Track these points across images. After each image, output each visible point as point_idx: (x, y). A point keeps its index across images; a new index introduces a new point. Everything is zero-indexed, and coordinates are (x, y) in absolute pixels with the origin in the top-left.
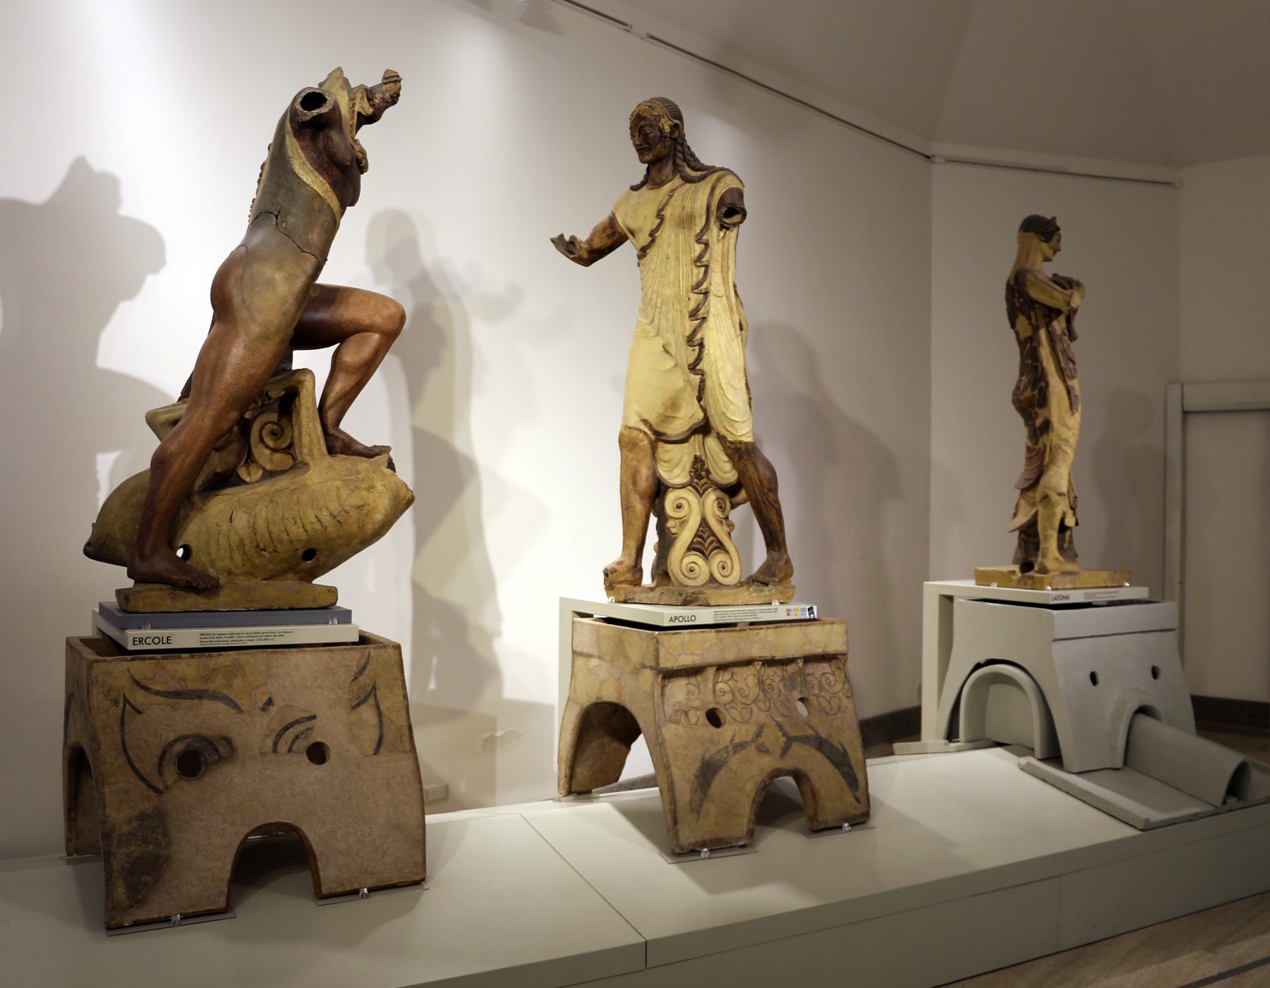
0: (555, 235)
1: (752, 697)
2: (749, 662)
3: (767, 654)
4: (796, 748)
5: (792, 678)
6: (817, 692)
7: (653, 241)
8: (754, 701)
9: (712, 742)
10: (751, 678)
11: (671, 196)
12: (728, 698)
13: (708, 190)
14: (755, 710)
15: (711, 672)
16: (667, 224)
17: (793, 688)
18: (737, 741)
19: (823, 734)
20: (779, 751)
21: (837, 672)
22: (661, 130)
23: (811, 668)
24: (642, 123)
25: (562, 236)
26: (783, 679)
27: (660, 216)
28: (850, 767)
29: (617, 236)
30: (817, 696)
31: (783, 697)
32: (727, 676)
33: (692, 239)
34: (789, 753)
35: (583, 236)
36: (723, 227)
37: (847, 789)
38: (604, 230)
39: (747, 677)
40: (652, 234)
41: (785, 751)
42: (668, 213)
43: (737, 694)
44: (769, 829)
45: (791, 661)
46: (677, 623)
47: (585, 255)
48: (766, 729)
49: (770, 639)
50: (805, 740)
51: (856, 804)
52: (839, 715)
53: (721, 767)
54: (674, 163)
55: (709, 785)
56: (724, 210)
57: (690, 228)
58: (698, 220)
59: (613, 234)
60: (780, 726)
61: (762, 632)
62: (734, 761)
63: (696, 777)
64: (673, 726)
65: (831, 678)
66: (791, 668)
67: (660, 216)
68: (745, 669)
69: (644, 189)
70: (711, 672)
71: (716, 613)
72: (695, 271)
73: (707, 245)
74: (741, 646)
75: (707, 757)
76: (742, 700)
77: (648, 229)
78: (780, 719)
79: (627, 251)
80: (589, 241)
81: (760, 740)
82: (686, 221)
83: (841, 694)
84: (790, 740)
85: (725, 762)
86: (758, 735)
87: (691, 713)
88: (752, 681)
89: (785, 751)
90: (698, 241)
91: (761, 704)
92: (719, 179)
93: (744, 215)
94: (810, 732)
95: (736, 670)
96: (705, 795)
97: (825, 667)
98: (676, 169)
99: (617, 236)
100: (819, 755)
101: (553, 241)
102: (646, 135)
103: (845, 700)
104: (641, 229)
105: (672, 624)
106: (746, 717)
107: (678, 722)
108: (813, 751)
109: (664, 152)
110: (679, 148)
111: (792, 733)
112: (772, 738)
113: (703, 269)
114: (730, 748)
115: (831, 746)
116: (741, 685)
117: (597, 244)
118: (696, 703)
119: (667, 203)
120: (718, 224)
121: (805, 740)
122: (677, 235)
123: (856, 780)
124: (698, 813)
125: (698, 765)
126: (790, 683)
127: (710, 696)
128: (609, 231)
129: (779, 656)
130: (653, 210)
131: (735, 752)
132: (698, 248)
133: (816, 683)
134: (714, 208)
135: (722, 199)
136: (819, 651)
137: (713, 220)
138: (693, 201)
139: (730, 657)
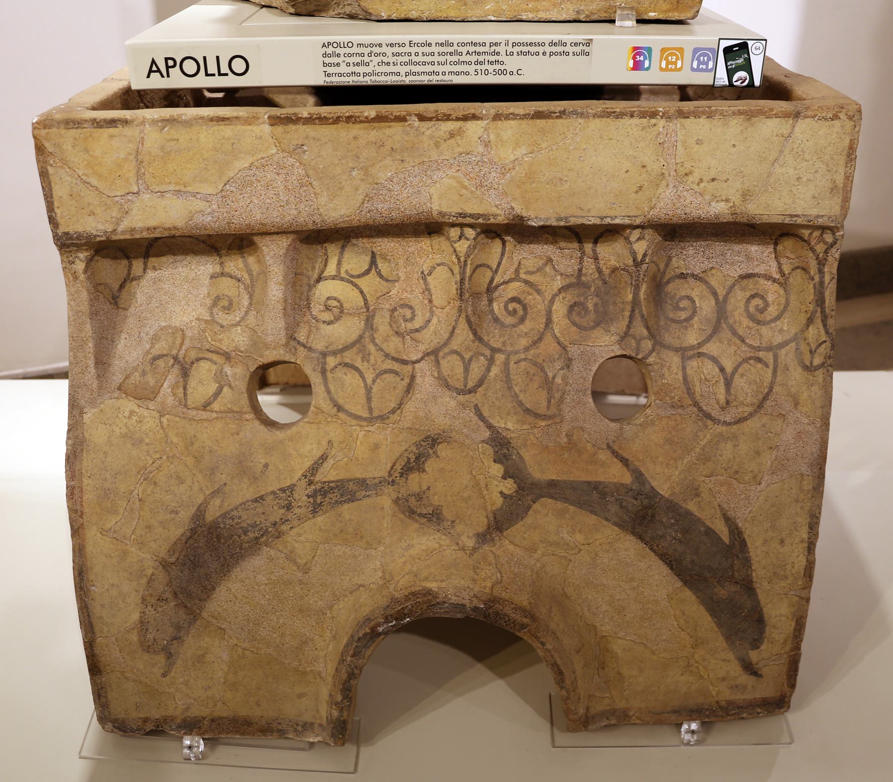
1: (429, 338)
2: (430, 227)
3: (496, 207)
4: (545, 516)
5: (608, 282)
6: (692, 338)
8: (434, 354)
9: (243, 468)
10: (441, 273)
12: (346, 330)
14: (426, 381)
15: (273, 254)
17: (603, 319)
18: (329, 473)
19: (664, 481)
20: (480, 522)
21: (797, 279)
23: (691, 257)
26: (577, 283)
28: (748, 587)
30: (686, 353)
31: (549, 346)
32: (354, 260)
34: (517, 531)
37: (719, 641)
39: (425, 274)
41: (499, 524)
43: (382, 322)
44: (479, 667)
45: (607, 232)
46: (177, 81)
48: (443, 450)
49: (508, 155)
50: (589, 497)
51: (745, 679)
52: (753, 424)
53: (256, 545)
55: (208, 590)
60: (501, 447)
61: (474, 129)
62: (305, 535)
63: (165, 565)
64: (129, 405)
65: (773, 292)
66: (611, 253)
68: (425, 243)
70: (273, 254)
71: (330, 50)
74: (384, 172)
75: (210, 517)
76: (393, 345)
78: (509, 425)
81: (415, 482)
83: (787, 355)
84: (526, 492)
85: (272, 533)
86: (414, 464)
87: (204, 371)
88: (443, 285)
89: (499, 524)
91: (452, 366)
94: (616, 474)
95: (384, 245)
96: (194, 616)
97: (759, 256)
100: (629, 546)
103: (797, 374)
105: (157, 82)
106: (384, 402)
107: (145, 395)
108: (610, 531)
111: (541, 469)
112: (469, 480)
114: (301, 496)
115: (687, 523)
116: (407, 290)
118: (238, 338)
121: (589, 497)
123: (759, 620)
124: (170, 656)
125: (176, 532)
126: (590, 302)
127: (274, 326)
129: (539, 214)
131: (316, 509)
133: (707, 307)
136: (718, 209)
139: (337, 210)
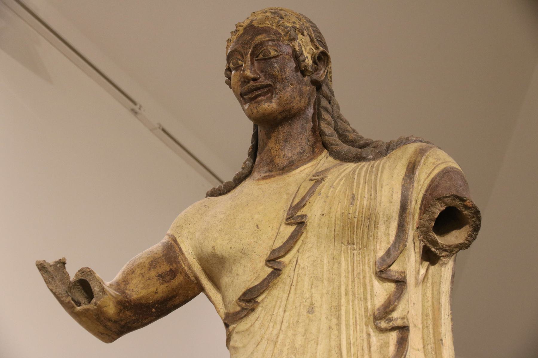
0: (51, 260)
7: (276, 273)
11: (318, 182)
13: (401, 170)
16: (310, 235)
22: (297, 57)
24: (260, 38)
25: (62, 263)
27: (297, 221)
29: (179, 279)
33: (369, 271)
35: (108, 276)
36: (429, 256)
38: (153, 263)
40: (275, 261)
42: (314, 211)
47: (111, 310)
54: (317, 132)
56: (438, 209)
57: (365, 246)
58: (382, 227)
59: (173, 273)
67: (297, 221)
69: (247, 185)
72: (376, 339)
73: (401, 283)
77: (263, 251)
79: (200, 315)
80: (119, 286)
82: (354, 229)
90: (382, 274)
92: (422, 152)
93: (476, 229)
98: (320, 143)
99: (179, 279)
101: (42, 267)
102: (267, 59)
104: (244, 253)
109: (298, 103)
110: (324, 102)
113: (394, 336)
117: (137, 291)
119: (311, 192)
120: (419, 245)
122: (335, 259)
128: (166, 267)
130: (279, 208)
132: (382, 291)
134: (415, 206)
135: (432, 188)
137: (411, 232)
138: (375, 188)
